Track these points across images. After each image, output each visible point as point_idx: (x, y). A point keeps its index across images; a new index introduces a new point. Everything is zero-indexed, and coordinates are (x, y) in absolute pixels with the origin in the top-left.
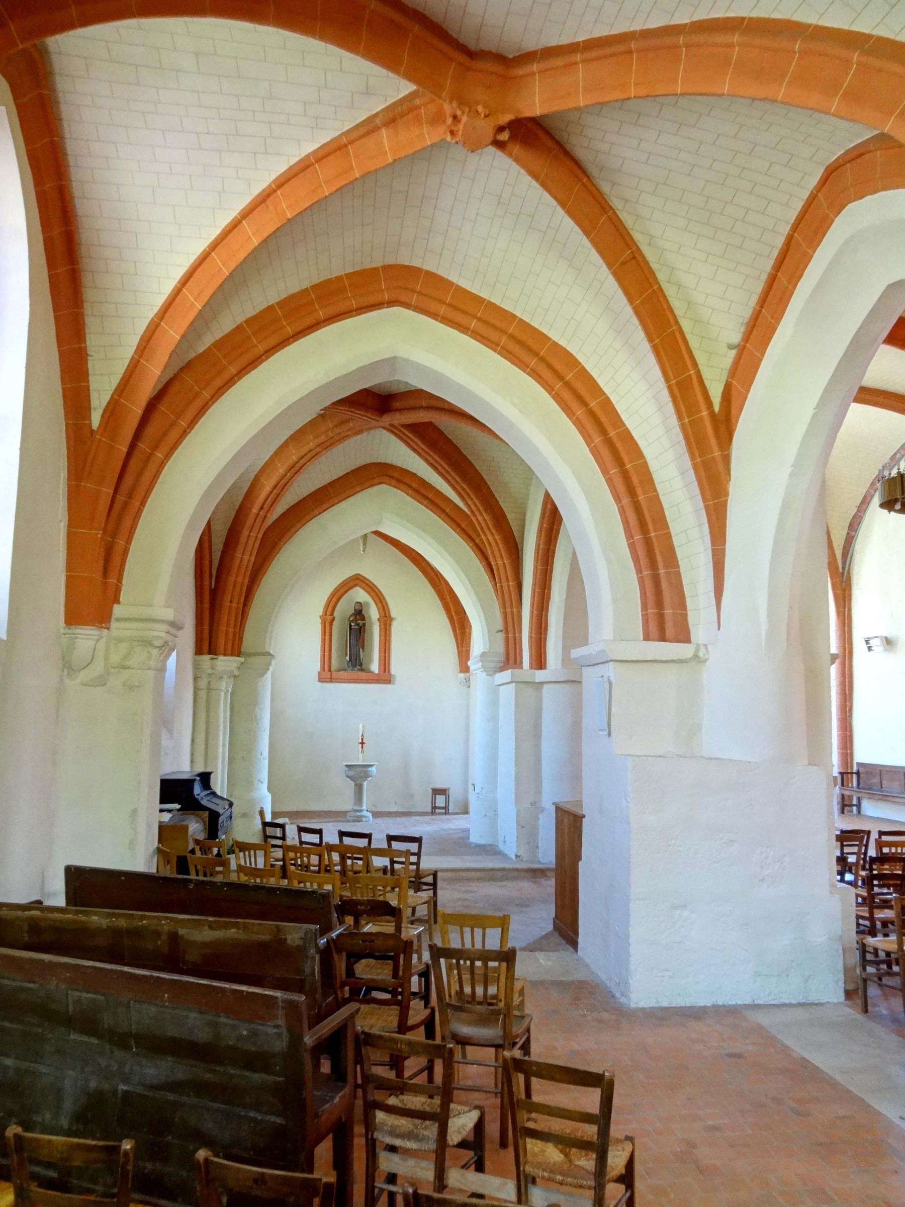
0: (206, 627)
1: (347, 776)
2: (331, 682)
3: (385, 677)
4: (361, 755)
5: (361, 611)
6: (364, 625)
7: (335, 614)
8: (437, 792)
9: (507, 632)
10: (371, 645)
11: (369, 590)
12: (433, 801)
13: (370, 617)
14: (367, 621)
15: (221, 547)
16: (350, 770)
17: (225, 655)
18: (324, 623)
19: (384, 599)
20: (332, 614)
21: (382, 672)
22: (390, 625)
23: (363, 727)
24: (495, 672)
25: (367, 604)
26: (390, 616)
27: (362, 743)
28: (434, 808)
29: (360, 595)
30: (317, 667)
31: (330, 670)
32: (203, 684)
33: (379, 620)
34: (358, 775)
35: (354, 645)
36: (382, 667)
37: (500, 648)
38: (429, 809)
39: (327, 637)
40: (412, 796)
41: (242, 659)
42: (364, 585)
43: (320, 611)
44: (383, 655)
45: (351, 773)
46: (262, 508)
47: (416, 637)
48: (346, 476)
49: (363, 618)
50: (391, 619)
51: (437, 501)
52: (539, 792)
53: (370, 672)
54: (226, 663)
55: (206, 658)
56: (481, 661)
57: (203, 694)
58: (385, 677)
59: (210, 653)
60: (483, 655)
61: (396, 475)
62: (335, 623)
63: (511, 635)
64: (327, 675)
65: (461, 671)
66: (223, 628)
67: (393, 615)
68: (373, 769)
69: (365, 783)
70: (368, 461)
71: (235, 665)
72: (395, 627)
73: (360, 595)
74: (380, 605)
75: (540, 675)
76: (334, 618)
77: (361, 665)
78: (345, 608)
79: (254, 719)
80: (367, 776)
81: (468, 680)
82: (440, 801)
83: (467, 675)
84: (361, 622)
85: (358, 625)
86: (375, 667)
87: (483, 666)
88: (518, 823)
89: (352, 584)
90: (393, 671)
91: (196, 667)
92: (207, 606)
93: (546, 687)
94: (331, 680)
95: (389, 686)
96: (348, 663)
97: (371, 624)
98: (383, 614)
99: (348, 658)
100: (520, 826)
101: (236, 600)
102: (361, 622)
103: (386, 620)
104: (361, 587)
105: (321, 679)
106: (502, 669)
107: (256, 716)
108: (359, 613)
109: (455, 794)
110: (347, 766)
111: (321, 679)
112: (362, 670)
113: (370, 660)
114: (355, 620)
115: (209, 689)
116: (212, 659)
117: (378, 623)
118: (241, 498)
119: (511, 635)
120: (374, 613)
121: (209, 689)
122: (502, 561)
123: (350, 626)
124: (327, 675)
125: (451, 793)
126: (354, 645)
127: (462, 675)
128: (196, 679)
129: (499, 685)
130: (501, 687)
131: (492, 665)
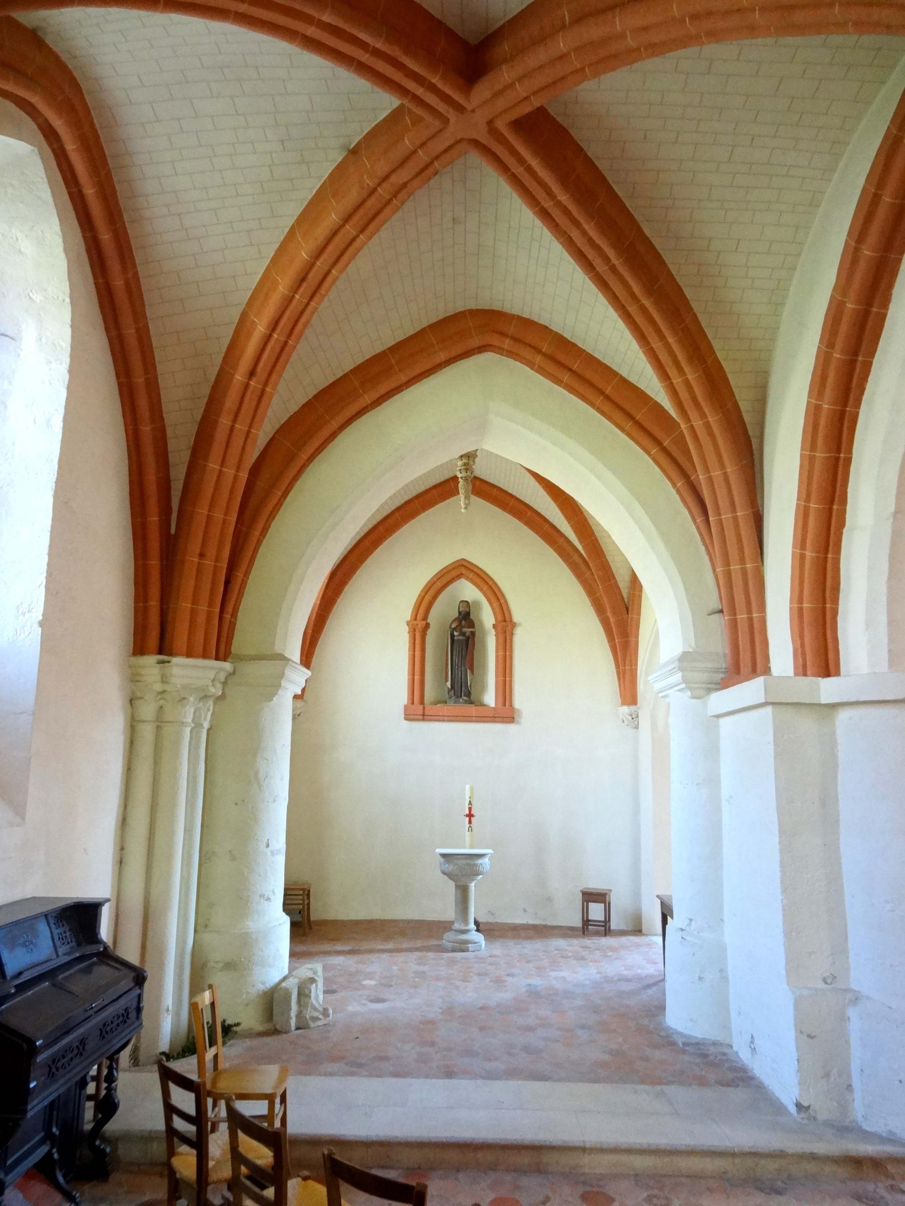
0: (154, 604)
1: (444, 873)
2: (423, 720)
3: (506, 713)
4: (468, 834)
5: (468, 614)
6: (473, 634)
7: (431, 619)
8: (590, 897)
9: (733, 612)
10: (484, 666)
11: (478, 580)
12: (585, 911)
13: (481, 622)
14: (477, 629)
15: (186, 456)
17: (189, 654)
18: (413, 632)
20: (425, 618)
21: (500, 706)
22: (512, 634)
23: (472, 789)
24: (709, 691)
25: (477, 604)
26: (511, 621)
27: (470, 816)
28: (586, 922)
29: (468, 591)
30: (402, 696)
31: (422, 702)
32: (147, 710)
33: (494, 626)
34: (461, 870)
35: (458, 664)
36: (501, 699)
37: (719, 644)
38: (577, 922)
39: (418, 653)
40: (550, 899)
41: (227, 666)
42: (471, 575)
43: (408, 615)
45: (449, 868)
46: (252, 373)
47: (551, 641)
48: (420, 335)
49: (471, 624)
50: (514, 625)
51: (588, 374)
52: (840, 949)
54: (189, 672)
55: (151, 660)
56: (681, 669)
57: (147, 732)
58: (506, 713)
59: (160, 652)
60: (684, 658)
61: (511, 330)
63: (742, 616)
64: (418, 709)
65: (623, 704)
66: (185, 605)
67: (516, 618)
68: (486, 861)
69: (473, 884)
70: (461, 306)
71: (212, 675)
73: (468, 591)
74: (496, 604)
75: (828, 689)
76: (427, 626)
77: (469, 694)
78: (443, 611)
79: (251, 780)
80: (474, 872)
81: (635, 717)
82: (596, 911)
83: (633, 708)
84: (467, 631)
85: (464, 634)
86: (490, 698)
87: (685, 680)
88: (800, 1031)
89: (454, 573)
91: (133, 678)
92: (154, 562)
93: (843, 716)
95: (511, 727)
96: (449, 691)
97: (484, 634)
98: (500, 618)
99: (449, 684)
100: (806, 1034)
101: (212, 551)
102: (467, 631)
103: (506, 626)
104: (467, 578)
105: (409, 716)
106: (724, 684)
107: (261, 774)
109: (620, 901)
110: (444, 856)
111: (409, 716)
112: (471, 703)
113: (483, 688)
114: (459, 627)
115: (160, 722)
116: (163, 662)
117: (493, 632)
118: (218, 360)
119: (742, 616)
120: (487, 617)
121: (160, 722)
122: (718, 471)
123: (452, 636)
124: (418, 709)
125: (614, 899)
126: (458, 664)
127: (626, 709)
128: (132, 701)
129: (718, 716)
130: (722, 721)
131: (705, 676)
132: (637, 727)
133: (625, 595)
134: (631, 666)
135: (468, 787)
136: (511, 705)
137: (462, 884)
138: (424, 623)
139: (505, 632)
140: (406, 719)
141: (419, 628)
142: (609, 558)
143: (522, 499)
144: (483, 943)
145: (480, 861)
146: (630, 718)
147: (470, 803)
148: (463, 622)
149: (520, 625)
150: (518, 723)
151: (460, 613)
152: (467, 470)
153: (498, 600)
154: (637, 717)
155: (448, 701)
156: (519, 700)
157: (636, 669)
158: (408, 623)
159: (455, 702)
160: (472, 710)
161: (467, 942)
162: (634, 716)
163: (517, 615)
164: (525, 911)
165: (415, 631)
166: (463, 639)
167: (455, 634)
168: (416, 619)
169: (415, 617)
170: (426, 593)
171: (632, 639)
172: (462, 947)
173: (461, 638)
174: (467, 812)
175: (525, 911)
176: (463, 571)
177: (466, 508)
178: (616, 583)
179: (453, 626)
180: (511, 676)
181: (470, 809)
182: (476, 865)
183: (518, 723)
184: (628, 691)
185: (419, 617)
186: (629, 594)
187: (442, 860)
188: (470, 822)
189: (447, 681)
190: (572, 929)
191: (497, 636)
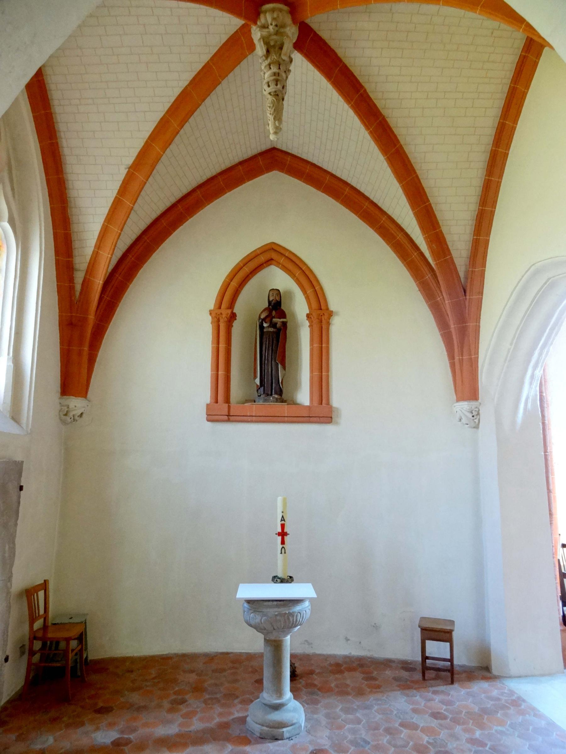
2: (229, 420)
3: (322, 412)
4: (280, 557)
6: (285, 324)
11: (290, 266)
13: (293, 315)
14: (288, 319)
16: (255, 611)
19: (318, 281)
21: (316, 403)
22: (328, 324)
25: (290, 294)
26: (327, 309)
27: (283, 534)
29: (278, 279)
30: (204, 394)
31: (227, 400)
33: (308, 316)
36: (316, 398)
39: (222, 346)
40: (376, 627)
42: (282, 260)
43: (211, 305)
44: (316, 373)
45: (257, 618)
49: (283, 315)
50: (331, 314)
53: (295, 403)
58: (322, 412)
62: (237, 327)
64: (223, 409)
65: (460, 398)
67: (332, 307)
69: (288, 637)
72: (337, 327)
73: (278, 279)
74: (310, 291)
76: (233, 316)
78: (251, 302)
81: (476, 415)
82: (437, 649)
83: (474, 404)
85: (273, 325)
86: (304, 396)
89: (262, 258)
90: (336, 400)
94: (229, 418)
97: (297, 327)
98: (315, 305)
99: (258, 381)
103: (321, 316)
104: (278, 264)
105: (212, 417)
108: (276, 306)
111: (212, 417)
112: (283, 401)
113: (296, 385)
114: (269, 317)
117: (307, 323)
120: (299, 307)
123: (261, 327)
124: (223, 409)
126: (269, 357)
127: (465, 405)
132: (477, 427)
133: (462, 275)
134: (470, 355)
135: (280, 499)
136: (328, 403)
137: (273, 638)
138: (229, 311)
139: (321, 321)
140: (208, 420)
141: (224, 319)
142: (444, 229)
143: (338, 174)
144: (303, 725)
145: (297, 608)
146: (470, 416)
147: (283, 519)
148: (274, 313)
149: (337, 314)
150: (337, 423)
151: (270, 302)
152: (277, 82)
153: (313, 287)
154: (478, 414)
155: (257, 400)
156: (337, 399)
157: (477, 358)
158: (211, 313)
159: (265, 401)
160: (284, 409)
161: (282, 725)
162: (475, 413)
163: (334, 301)
164: (347, 640)
165: (219, 320)
166: (274, 333)
167: (265, 325)
168: (220, 308)
169: (219, 305)
170: (231, 280)
171: (471, 324)
172: (273, 733)
173: (271, 330)
174: (279, 530)
175: (347, 640)
176: (274, 255)
177: (276, 133)
178: (452, 259)
179: (262, 317)
180: (328, 371)
181: (283, 526)
182: (292, 614)
183: (337, 423)
184: (466, 384)
185: (223, 306)
186: (467, 272)
187: (246, 605)
188: (283, 542)
189: (255, 377)
190: (406, 666)
191: (311, 326)
